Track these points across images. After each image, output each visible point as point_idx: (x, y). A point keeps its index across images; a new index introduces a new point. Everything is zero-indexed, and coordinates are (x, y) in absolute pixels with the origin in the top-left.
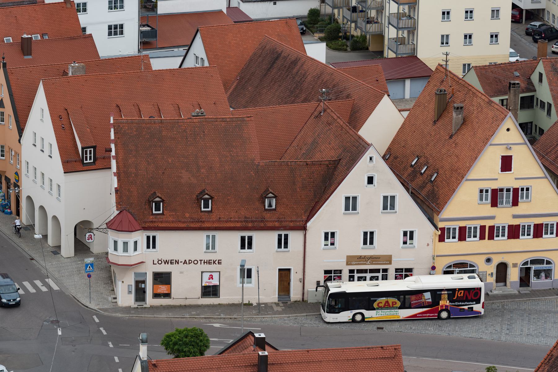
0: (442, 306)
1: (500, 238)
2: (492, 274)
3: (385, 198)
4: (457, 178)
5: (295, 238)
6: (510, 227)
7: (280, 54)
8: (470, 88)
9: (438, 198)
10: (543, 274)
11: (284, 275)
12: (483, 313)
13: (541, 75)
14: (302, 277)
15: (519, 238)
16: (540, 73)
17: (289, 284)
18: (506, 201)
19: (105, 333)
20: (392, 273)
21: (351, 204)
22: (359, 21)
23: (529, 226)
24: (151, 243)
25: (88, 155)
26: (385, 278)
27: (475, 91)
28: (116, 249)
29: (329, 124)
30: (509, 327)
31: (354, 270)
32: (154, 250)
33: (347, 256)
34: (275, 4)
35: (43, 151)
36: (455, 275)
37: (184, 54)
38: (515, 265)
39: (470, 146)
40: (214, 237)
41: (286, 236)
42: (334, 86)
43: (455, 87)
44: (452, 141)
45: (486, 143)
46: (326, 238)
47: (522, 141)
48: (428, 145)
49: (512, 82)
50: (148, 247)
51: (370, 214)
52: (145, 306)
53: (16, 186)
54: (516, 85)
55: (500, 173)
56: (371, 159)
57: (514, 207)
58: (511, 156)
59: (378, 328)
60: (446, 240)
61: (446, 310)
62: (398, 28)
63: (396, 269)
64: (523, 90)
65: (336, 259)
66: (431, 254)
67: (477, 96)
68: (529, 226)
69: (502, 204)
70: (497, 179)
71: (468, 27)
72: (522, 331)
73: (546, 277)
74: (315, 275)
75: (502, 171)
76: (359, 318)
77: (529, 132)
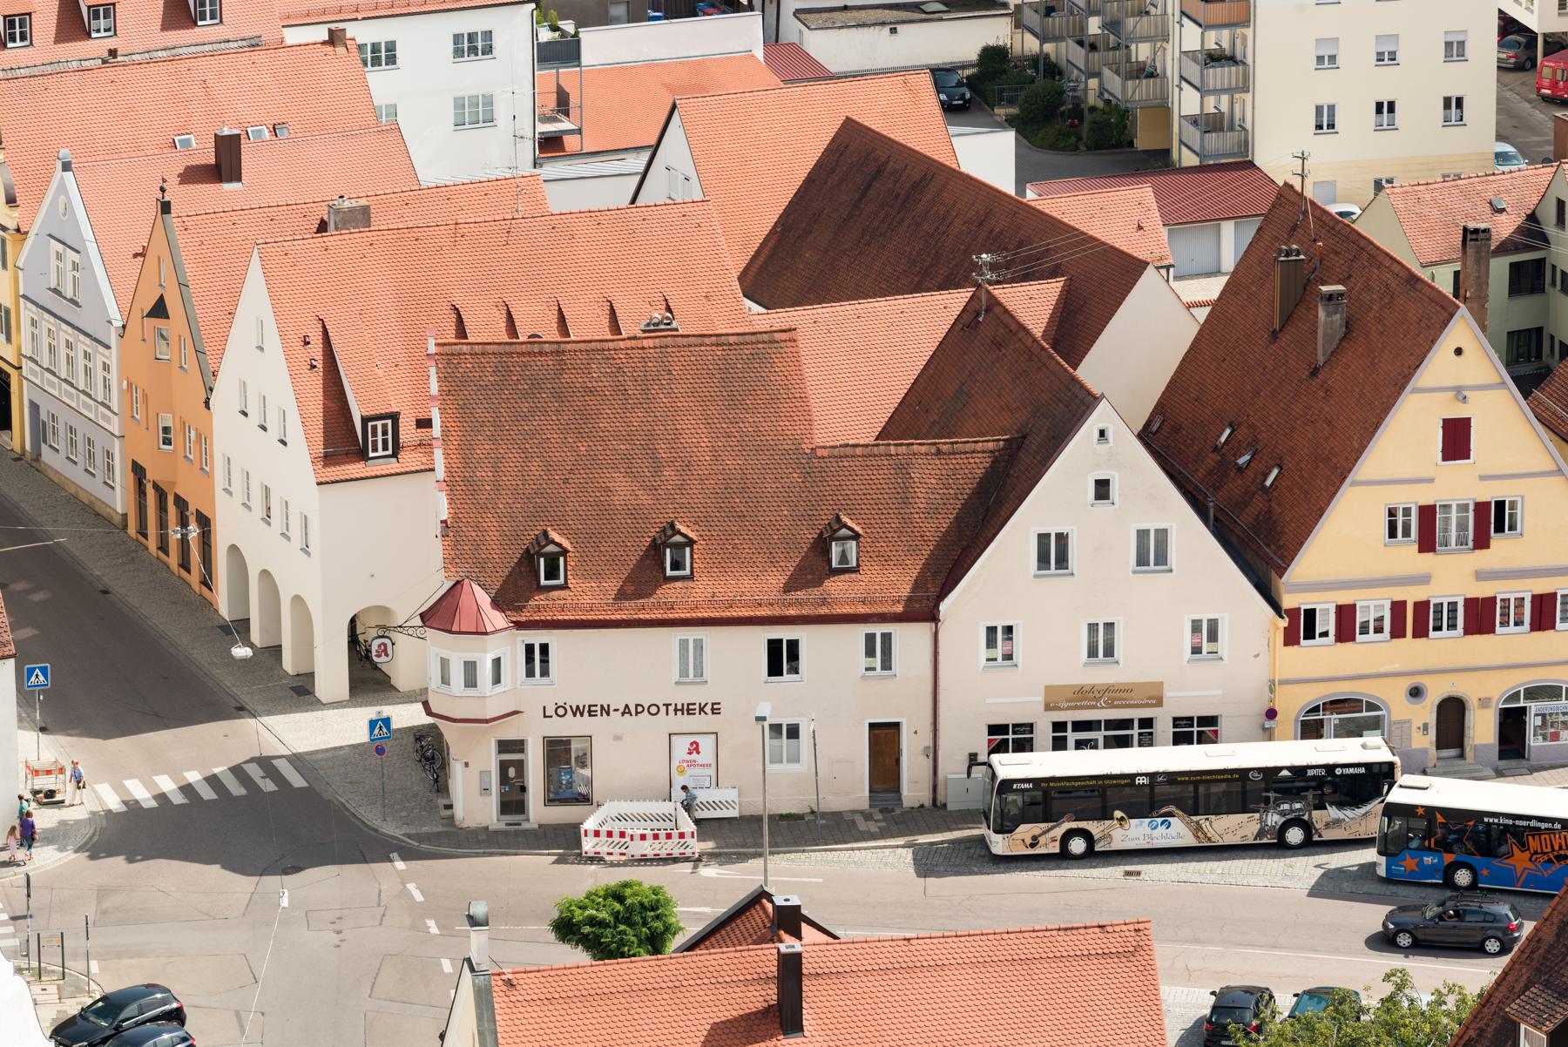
2: (1426, 727)
3: (1142, 535)
5: (910, 639)
7: (885, 164)
8: (1362, 243)
9: (1283, 532)
11: (884, 737)
14: (931, 744)
15: (1492, 631)
17: (898, 761)
19: (419, 897)
20: (1164, 728)
21: (1053, 553)
22: (1107, 72)
23: (1520, 602)
24: (537, 660)
25: (380, 438)
26: (1147, 740)
28: (445, 680)
29: (999, 345)
31: (1065, 724)
32: (545, 679)
33: (1047, 688)
34: (893, 31)
35: (264, 428)
37: (641, 169)
40: (699, 645)
41: (887, 638)
42: (1020, 244)
44: (1316, 382)
45: (1403, 387)
46: (991, 643)
48: (1256, 394)
49: (1472, 225)
50: (530, 673)
51: (1103, 576)
52: (525, 826)
53: (204, 522)
54: (1482, 235)
56: (1102, 433)
57: (1478, 552)
58: (1469, 420)
59: (1128, 874)
62: (1203, 91)
63: (1175, 719)
65: (1018, 700)
66: (1265, 677)
70: (1431, 480)
71: (1386, 85)
74: (963, 736)
75: (1445, 458)
76: (1078, 846)
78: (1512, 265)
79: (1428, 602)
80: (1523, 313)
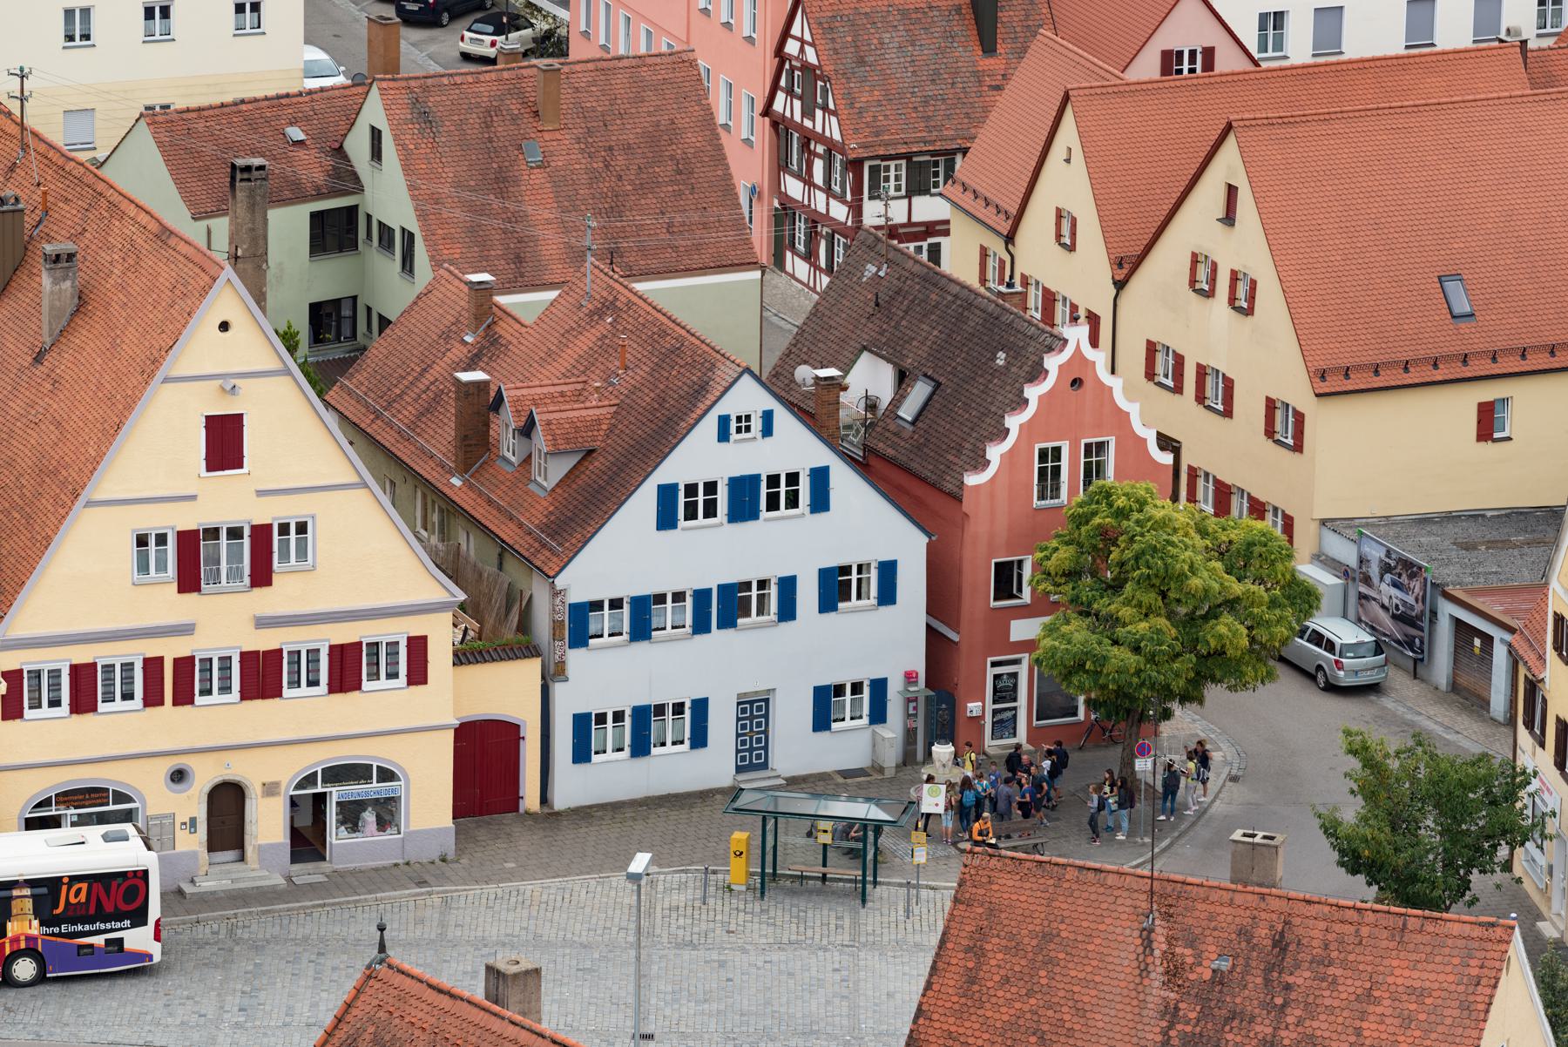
0: (16, 940)
1: (216, 697)
2: (193, 821)
4: (56, 498)
6: (245, 656)
10: (369, 817)
12: (157, 958)
13: (376, 135)
15: (280, 695)
16: (373, 128)
18: (230, 570)
27: (116, 198)
30: (246, 1002)
36: (66, 833)
38: (270, 789)
39: (99, 386)
43: (55, 186)
44: (41, 370)
45: (151, 375)
47: (274, 364)
49: (240, 162)
54: (256, 174)
55: (204, 473)
57: (257, 590)
60: (28, 713)
61: (31, 952)
64: (318, 188)
67: (123, 215)
68: (313, 654)
69: (217, 581)
72: (290, 1012)
73: (382, 824)
75: (209, 469)
77: (346, 331)
78: (316, 217)
79: (193, 658)
80: (329, 279)
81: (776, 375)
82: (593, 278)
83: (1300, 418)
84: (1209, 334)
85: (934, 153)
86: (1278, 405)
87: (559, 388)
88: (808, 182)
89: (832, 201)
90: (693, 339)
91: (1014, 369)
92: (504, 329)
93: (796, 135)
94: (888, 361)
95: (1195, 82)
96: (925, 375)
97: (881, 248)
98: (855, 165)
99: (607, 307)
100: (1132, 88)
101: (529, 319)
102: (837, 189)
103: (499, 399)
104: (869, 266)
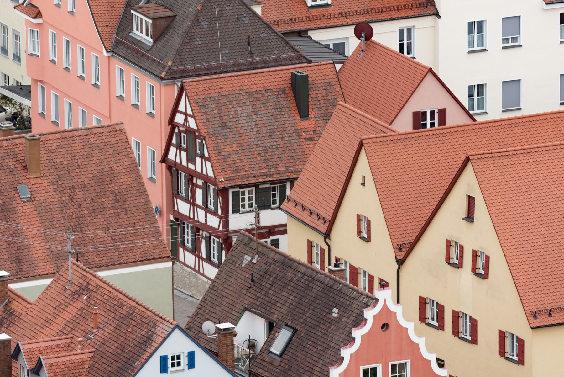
81: (189, 328)
82: (72, 271)
83: (521, 343)
84: (460, 291)
85: (272, 182)
86: (507, 335)
87: (55, 343)
88: (193, 203)
89: (208, 215)
90: (140, 308)
91: (344, 319)
92: (16, 306)
93: (183, 174)
94: (262, 316)
95: (427, 133)
96: (287, 325)
97: (254, 245)
98: (223, 192)
99: (83, 289)
100: (403, 137)
101: (32, 298)
102: (212, 207)
103: (18, 350)
104: (246, 257)
